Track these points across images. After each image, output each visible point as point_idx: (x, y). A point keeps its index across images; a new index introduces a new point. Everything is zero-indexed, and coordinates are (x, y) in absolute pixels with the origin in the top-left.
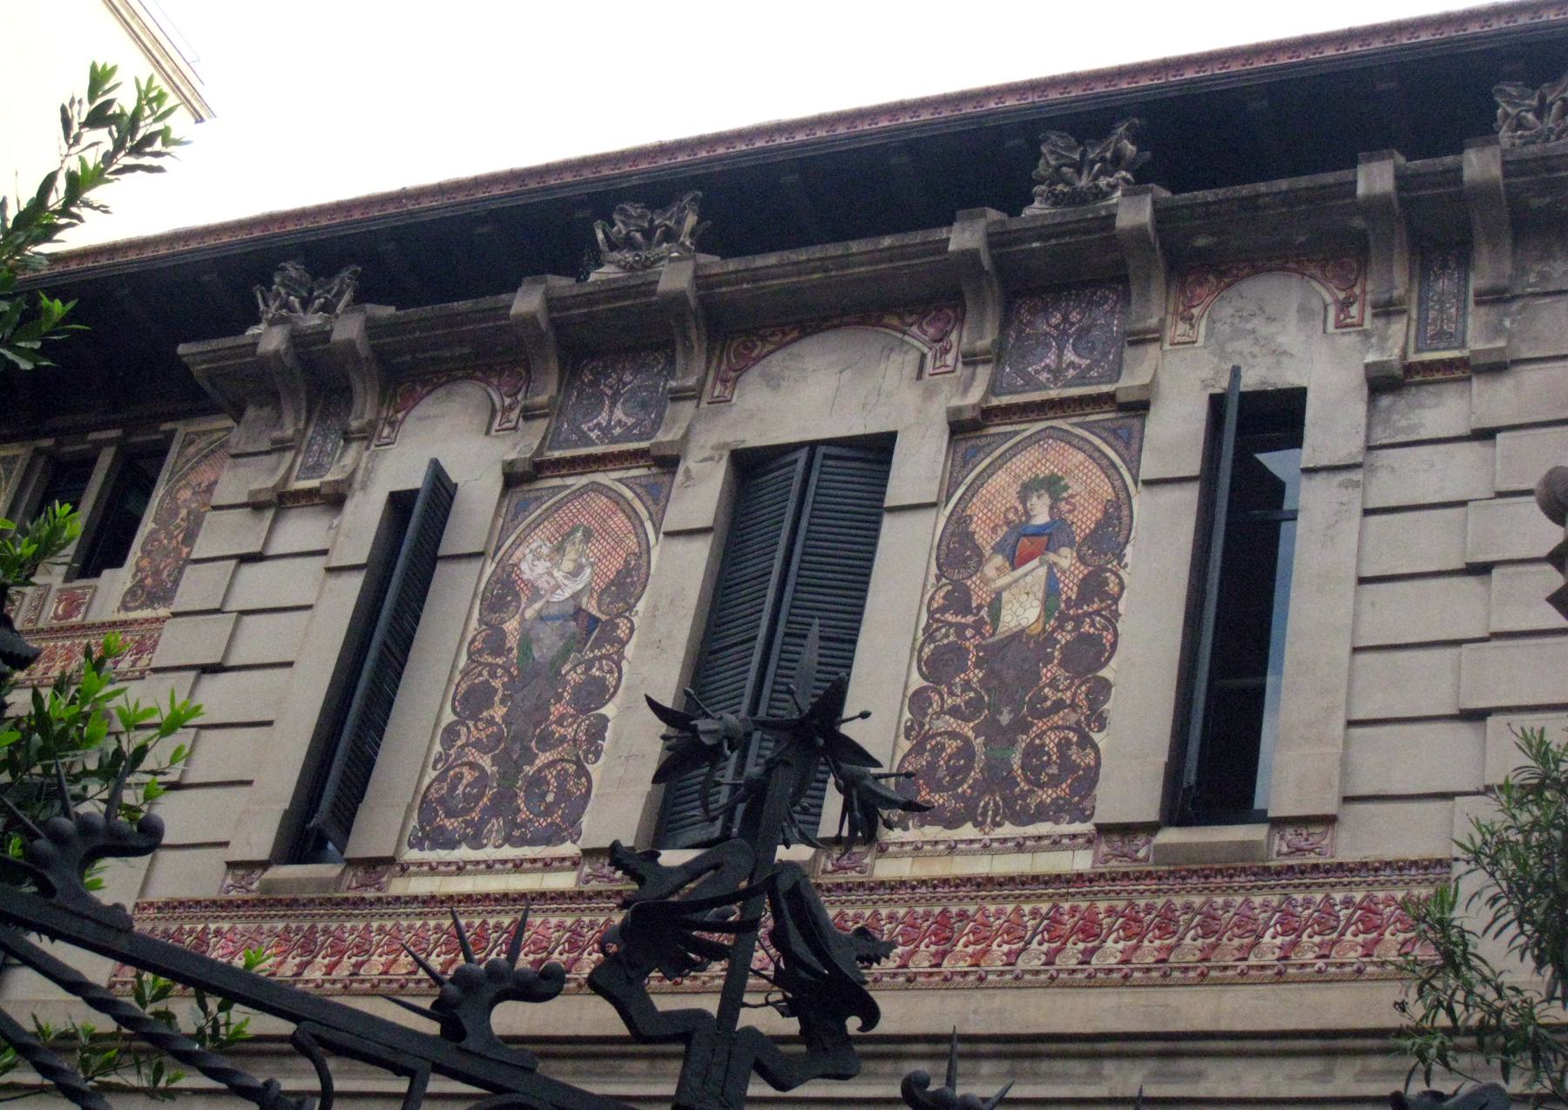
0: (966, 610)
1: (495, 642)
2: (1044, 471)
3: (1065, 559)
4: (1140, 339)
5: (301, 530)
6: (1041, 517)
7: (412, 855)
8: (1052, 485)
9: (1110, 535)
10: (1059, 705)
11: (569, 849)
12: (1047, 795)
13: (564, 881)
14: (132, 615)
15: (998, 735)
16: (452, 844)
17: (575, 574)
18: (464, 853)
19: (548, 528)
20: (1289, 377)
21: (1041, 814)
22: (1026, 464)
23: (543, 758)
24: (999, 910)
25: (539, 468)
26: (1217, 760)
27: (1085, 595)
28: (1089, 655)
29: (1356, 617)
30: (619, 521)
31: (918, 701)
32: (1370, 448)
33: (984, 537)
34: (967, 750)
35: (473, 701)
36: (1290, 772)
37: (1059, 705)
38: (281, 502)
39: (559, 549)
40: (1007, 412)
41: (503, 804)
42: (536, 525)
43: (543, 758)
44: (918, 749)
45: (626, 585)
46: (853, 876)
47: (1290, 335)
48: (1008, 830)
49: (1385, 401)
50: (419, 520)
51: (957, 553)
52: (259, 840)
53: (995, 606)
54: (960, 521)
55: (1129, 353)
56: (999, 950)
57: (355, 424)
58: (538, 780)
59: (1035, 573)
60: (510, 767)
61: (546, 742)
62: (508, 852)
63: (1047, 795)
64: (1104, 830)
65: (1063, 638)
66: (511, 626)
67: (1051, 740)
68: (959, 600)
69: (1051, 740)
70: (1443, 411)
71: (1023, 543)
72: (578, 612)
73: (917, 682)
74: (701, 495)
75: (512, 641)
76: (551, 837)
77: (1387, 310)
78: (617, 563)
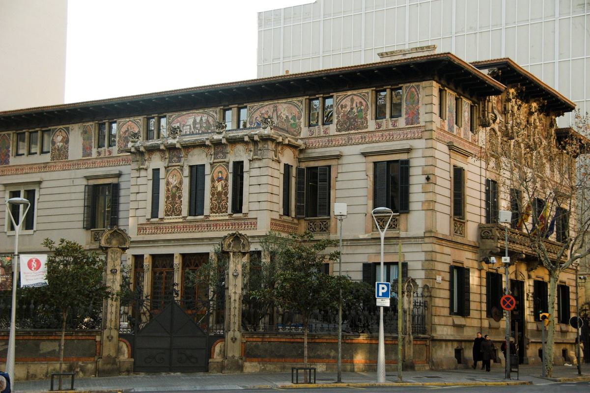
0: (214, 188)
1: (168, 190)
2: (220, 170)
3: (223, 182)
4: (227, 153)
5: (143, 173)
6: (220, 177)
7: (166, 217)
8: (221, 172)
9: (227, 180)
10: (224, 200)
11: (181, 216)
12: (224, 210)
13: (181, 220)
14: (120, 155)
15: (219, 203)
16: (169, 216)
17: (175, 181)
18: (170, 217)
19: (171, 175)
20: (241, 160)
21: (223, 212)
22: (218, 169)
23: (176, 205)
24: (220, 223)
25: (168, 167)
26: (237, 206)
27: (225, 187)
28: (226, 194)
29: (249, 190)
30: (178, 174)
31: (211, 199)
32: (250, 169)
33: (215, 179)
34: (216, 205)
35: (168, 198)
36: (245, 209)
37: (224, 200)
38: (139, 170)
39: (173, 178)
40: (215, 163)
41: (173, 211)
42: (170, 174)
43: (176, 205)
44: (212, 205)
45: (181, 183)
46: (208, 219)
47: (242, 153)
48: (221, 214)
49: (251, 162)
50: (156, 171)
51: (213, 181)
52: (149, 216)
53: (217, 187)
54: (213, 177)
55: (227, 155)
56: (221, 227)
57: (146, 159)
58: (176, 208)
59: (220, 183)
60: (173, 207)
61: (176, 203)
62: (175, 217)
63: (224, 210)
64: (229, 214)
65: (224, 192)
66: (170, 188)
67: (223, 204)
68: (213, 187)
69: (223, 204)
70: (256, 164)
71: (219, 180)
72: (176, 186)
73: (211, 197)
74: (186, 172)
75: (170, 190)
76: (179, 215)
77: (251, 151)
78: (179, 180)
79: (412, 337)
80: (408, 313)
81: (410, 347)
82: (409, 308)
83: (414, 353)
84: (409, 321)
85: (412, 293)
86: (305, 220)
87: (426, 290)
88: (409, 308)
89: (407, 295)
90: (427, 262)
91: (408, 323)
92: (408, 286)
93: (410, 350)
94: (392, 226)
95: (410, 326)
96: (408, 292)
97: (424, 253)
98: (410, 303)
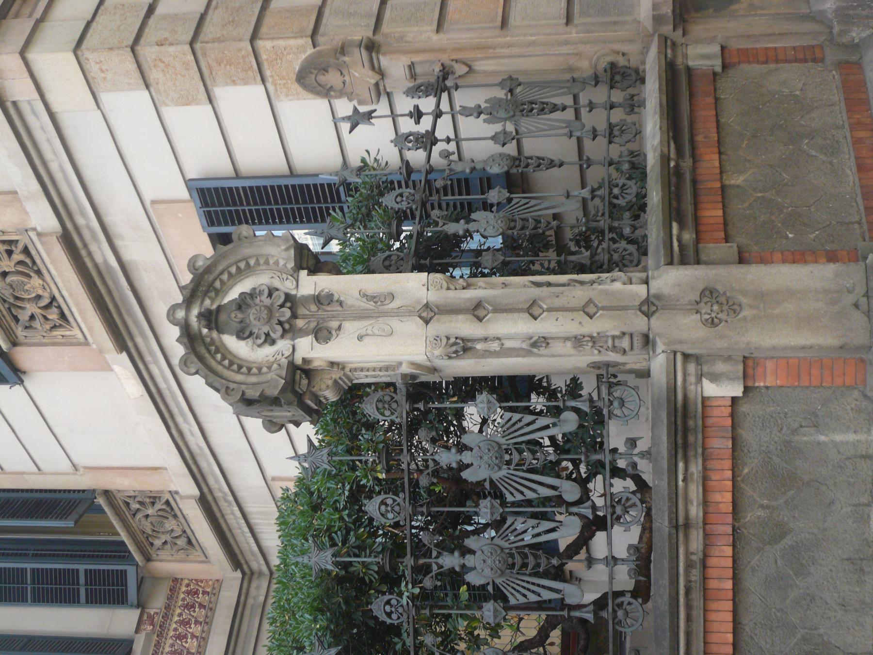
79: (670, 280)
80: (464, 327)
81: (762, 297)
82: (428, 313)
83: (798, 257)
84: (532, 310)
85: (309, 284)
86: (148, 559)
87: (332, 78)
88: (428, 313)
89: (322, 334)
90: (154, 75)
91: (546, 326)
92: (243, 334)
93: (789, 294)
94: (20, 263)
95: (578, 295)
96: (289, 330)
97: (105, 98)
98: (378, 306)
